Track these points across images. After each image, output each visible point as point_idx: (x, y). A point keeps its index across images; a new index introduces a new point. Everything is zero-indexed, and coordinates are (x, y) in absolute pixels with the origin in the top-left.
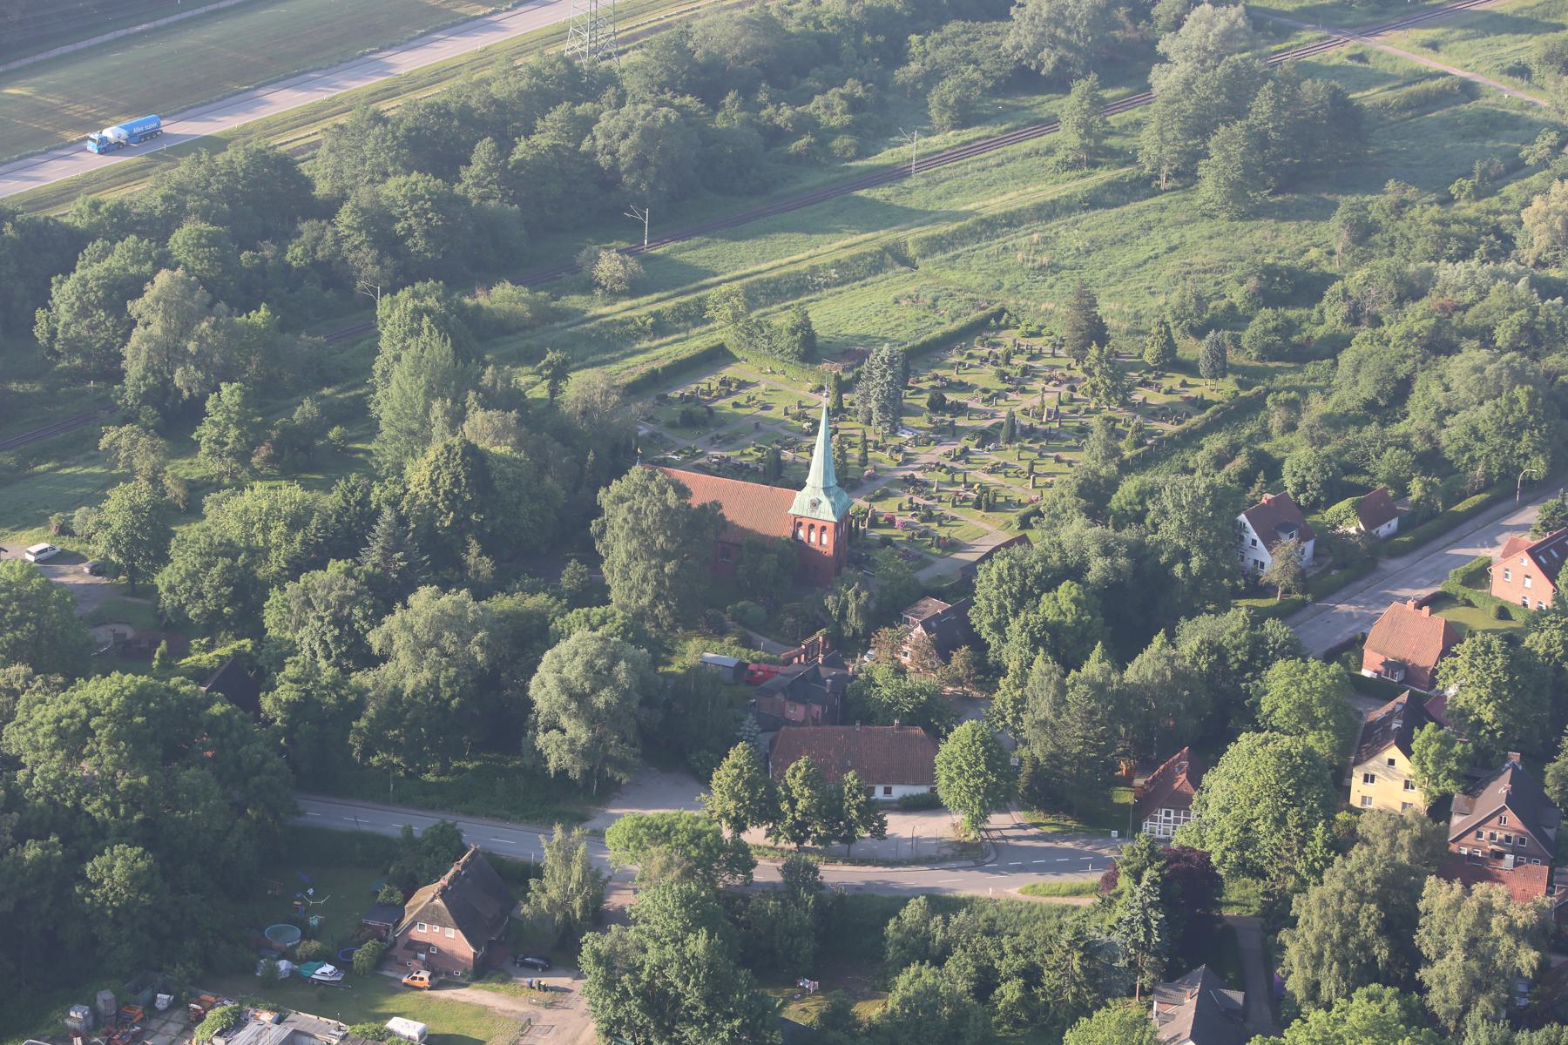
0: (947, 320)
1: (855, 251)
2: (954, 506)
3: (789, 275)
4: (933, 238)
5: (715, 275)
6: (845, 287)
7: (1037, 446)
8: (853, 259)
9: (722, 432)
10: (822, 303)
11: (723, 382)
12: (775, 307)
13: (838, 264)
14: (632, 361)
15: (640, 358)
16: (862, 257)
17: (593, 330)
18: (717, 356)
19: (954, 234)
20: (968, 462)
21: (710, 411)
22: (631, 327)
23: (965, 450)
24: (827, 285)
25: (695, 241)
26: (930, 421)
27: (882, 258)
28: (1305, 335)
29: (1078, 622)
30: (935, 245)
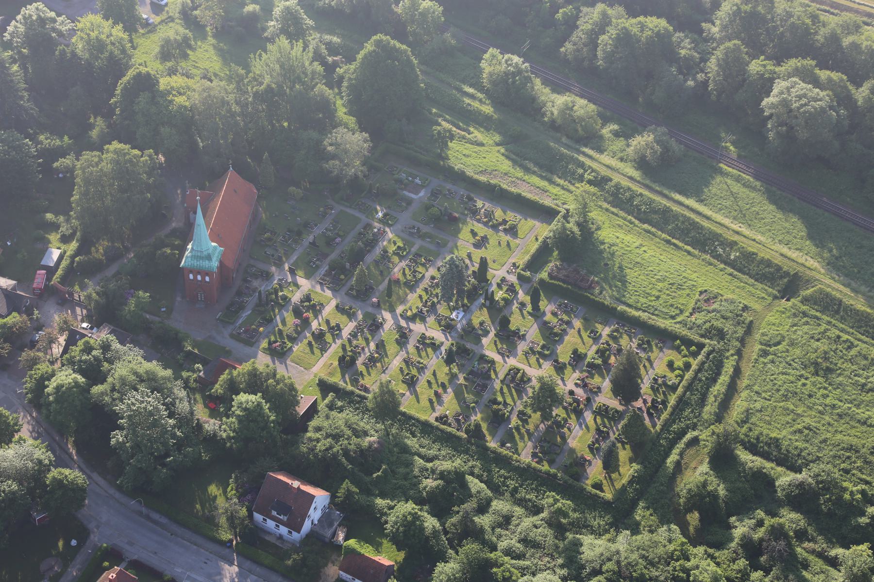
0: (679, 319)
1: (778, 260)
2: (344, 347)
3: (711, 232)
4: (833, 299)
5: (701, 201)
6: (722, 266)
7: (461, 380)
8: (762, 261)
9: (425, 229)
10: (689, 257)
11: (505, 222)
12: (664, 235)
13: (749, 257)
14: (535, 180)
15: (544, 184)
16: (768, 263)
17: (562, 155)
18: (547, 214)
19: (857, 312)
20: (417, 348)
21: (454, 220)
22: (580, 171)
23: (435, 347)
24: (718, 257)
25: (758, 184)
26: (481, 324)
27: (781, 277)
28: (737, 524)
29: (49, 395)
30: (828, 304)
